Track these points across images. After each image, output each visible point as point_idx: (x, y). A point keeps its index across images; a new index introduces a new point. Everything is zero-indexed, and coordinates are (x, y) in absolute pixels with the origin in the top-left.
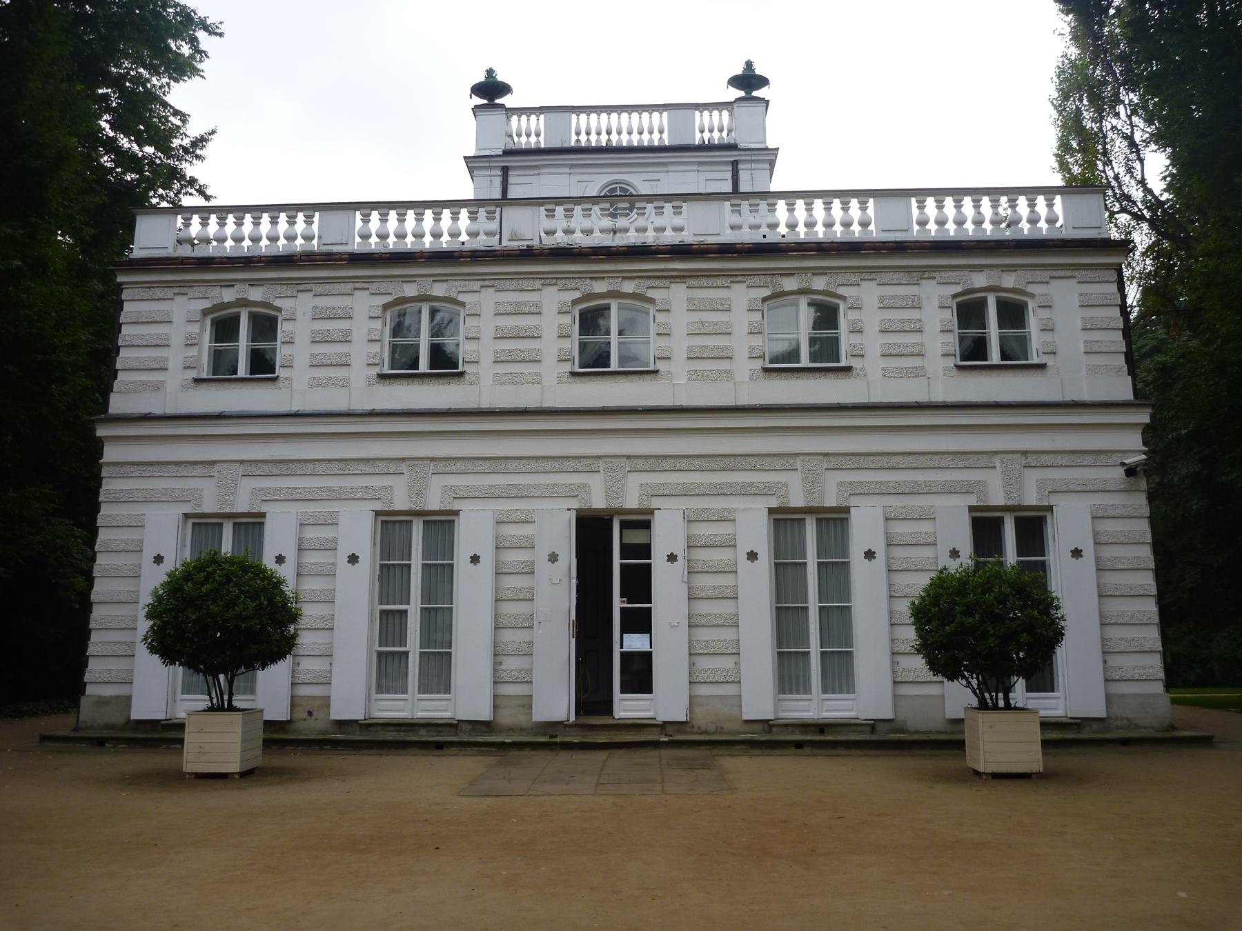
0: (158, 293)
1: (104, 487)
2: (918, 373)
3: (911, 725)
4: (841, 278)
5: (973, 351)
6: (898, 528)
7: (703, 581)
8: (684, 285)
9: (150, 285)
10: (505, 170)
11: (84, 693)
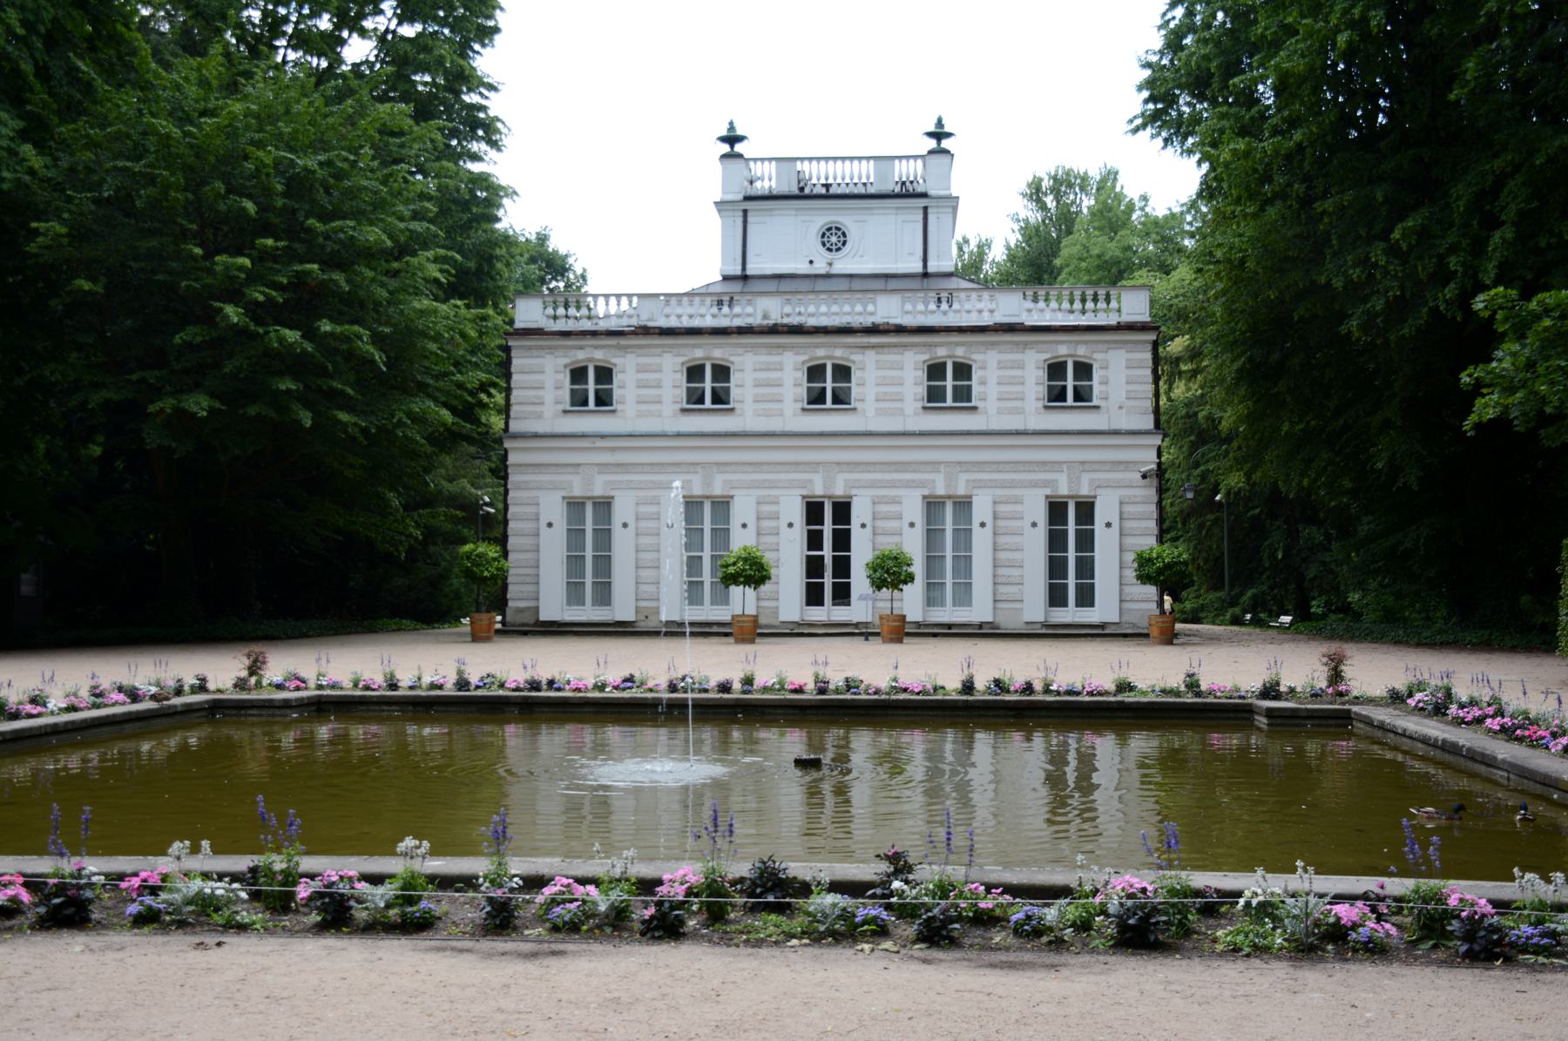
0: (535, 353)
2: (1019, 411)
3: (1002, 625)
5: (1056, 395)
9: (530, 348)
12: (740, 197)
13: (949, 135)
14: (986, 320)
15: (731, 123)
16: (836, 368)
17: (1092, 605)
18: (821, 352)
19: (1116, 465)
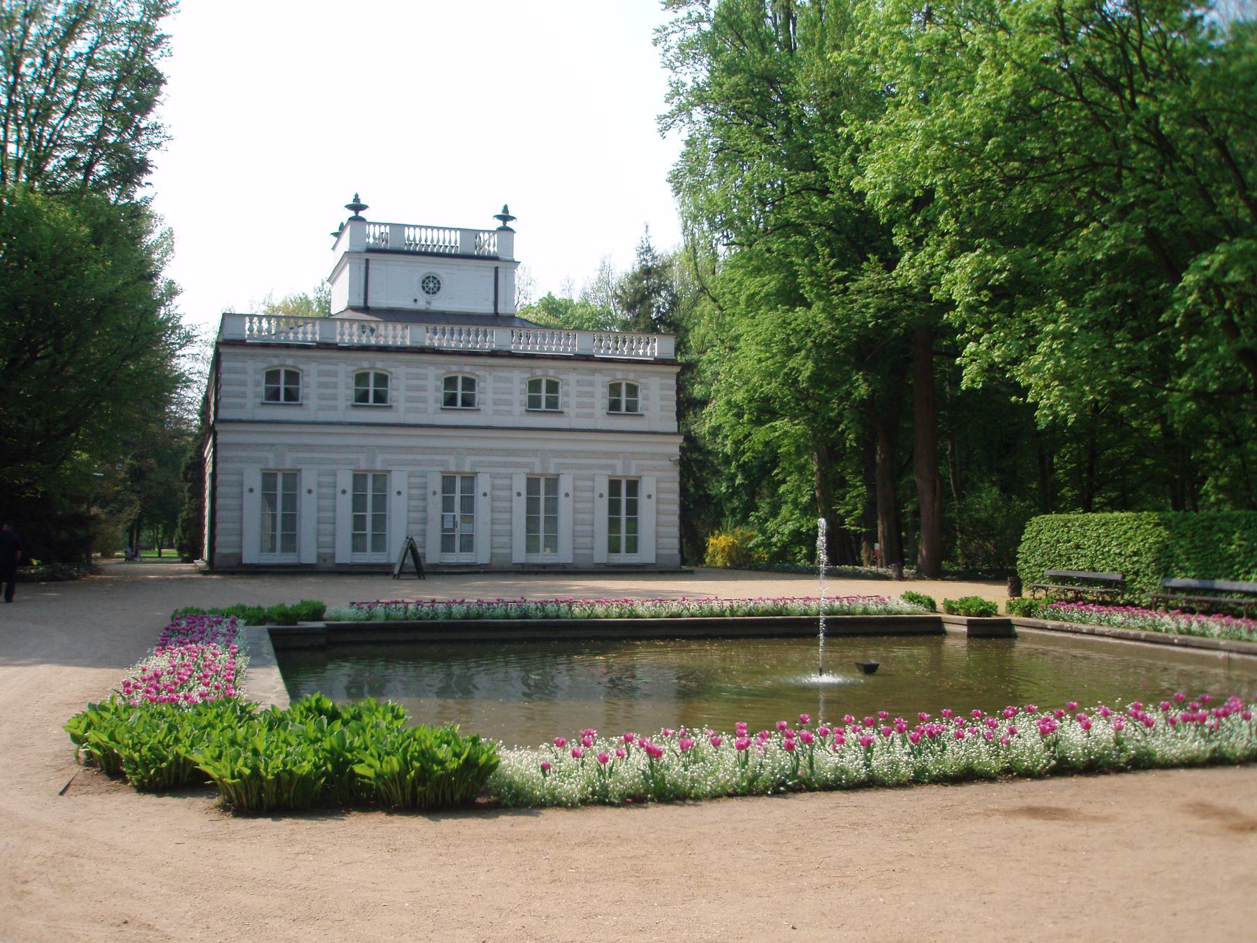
2: (591, 416)
6: (579, 483)
7: (498, 504)
12: (364, 249)
13: (513, 218)
14: (569, 352)
15: (356, 195)
16: (465, 380)
18: (454, 368)
19: (653, 456)
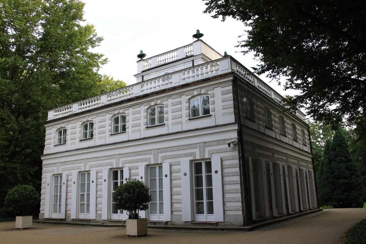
1: (43, 170)
3: (175, 224)
4: (163, 100)
8: (131, 108)
10: (143, 76)
11: (40, 213)
17: (213, 213)
19: (218, 142)
